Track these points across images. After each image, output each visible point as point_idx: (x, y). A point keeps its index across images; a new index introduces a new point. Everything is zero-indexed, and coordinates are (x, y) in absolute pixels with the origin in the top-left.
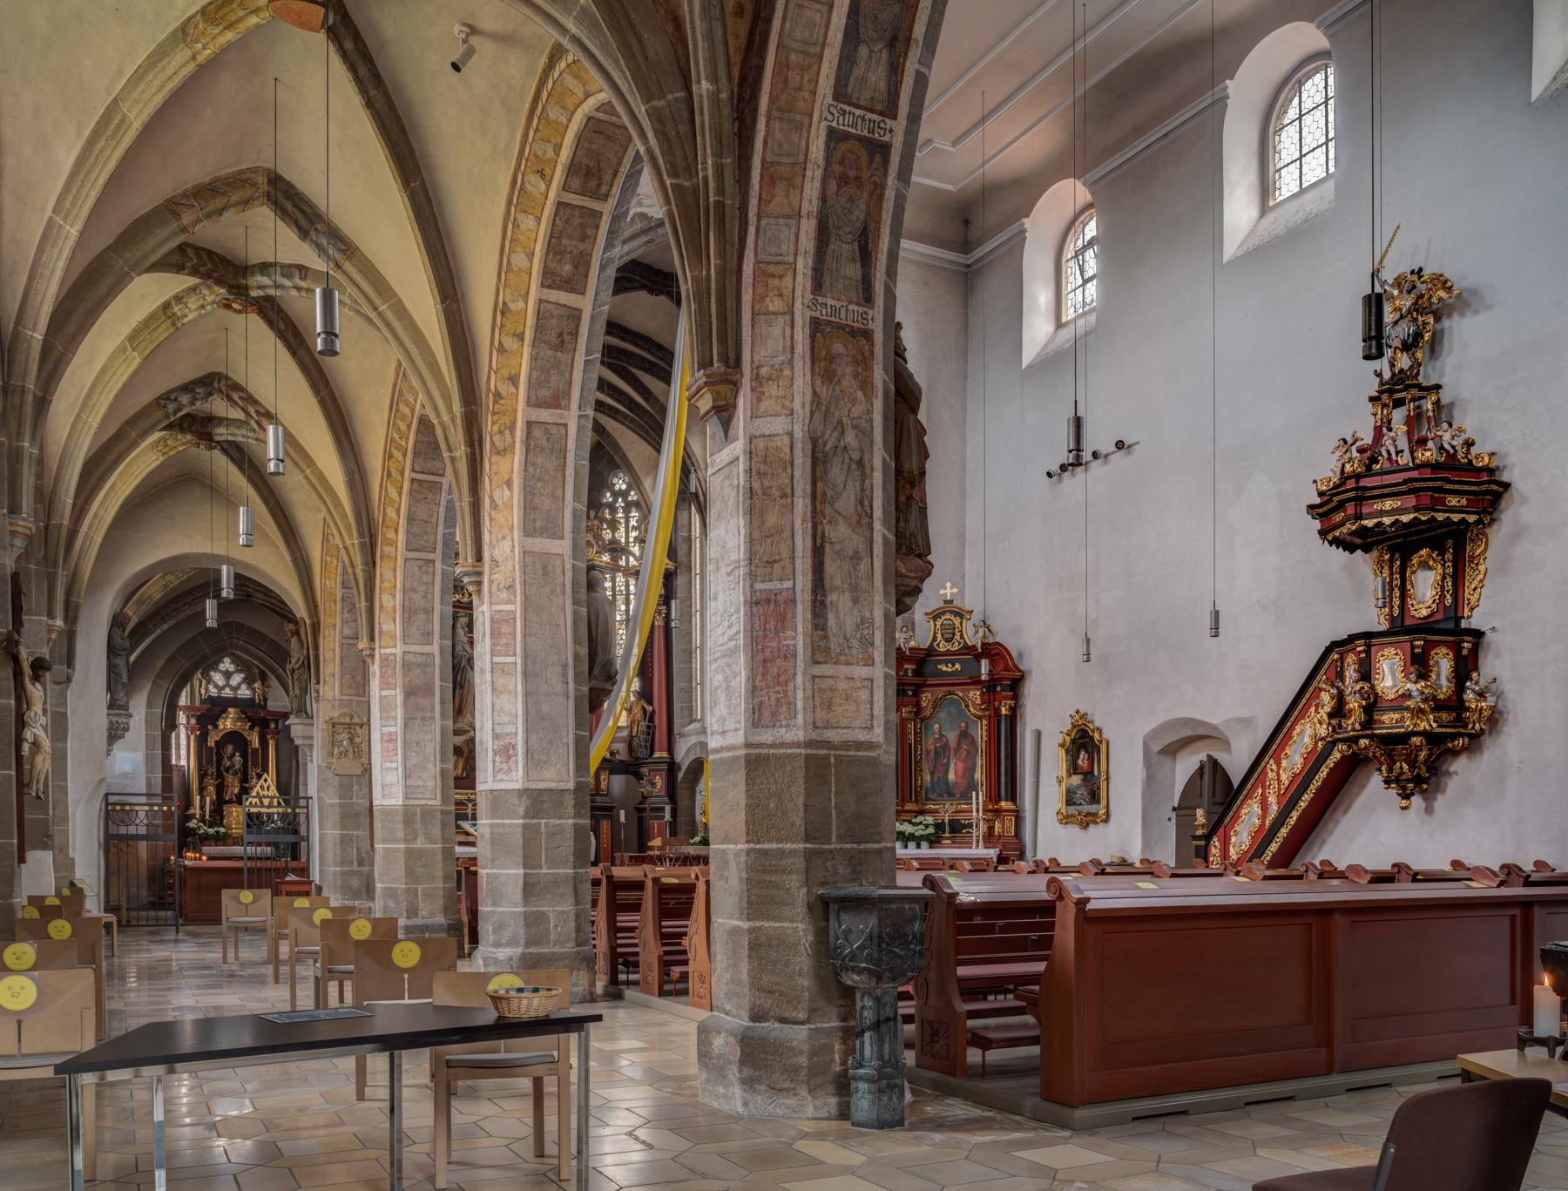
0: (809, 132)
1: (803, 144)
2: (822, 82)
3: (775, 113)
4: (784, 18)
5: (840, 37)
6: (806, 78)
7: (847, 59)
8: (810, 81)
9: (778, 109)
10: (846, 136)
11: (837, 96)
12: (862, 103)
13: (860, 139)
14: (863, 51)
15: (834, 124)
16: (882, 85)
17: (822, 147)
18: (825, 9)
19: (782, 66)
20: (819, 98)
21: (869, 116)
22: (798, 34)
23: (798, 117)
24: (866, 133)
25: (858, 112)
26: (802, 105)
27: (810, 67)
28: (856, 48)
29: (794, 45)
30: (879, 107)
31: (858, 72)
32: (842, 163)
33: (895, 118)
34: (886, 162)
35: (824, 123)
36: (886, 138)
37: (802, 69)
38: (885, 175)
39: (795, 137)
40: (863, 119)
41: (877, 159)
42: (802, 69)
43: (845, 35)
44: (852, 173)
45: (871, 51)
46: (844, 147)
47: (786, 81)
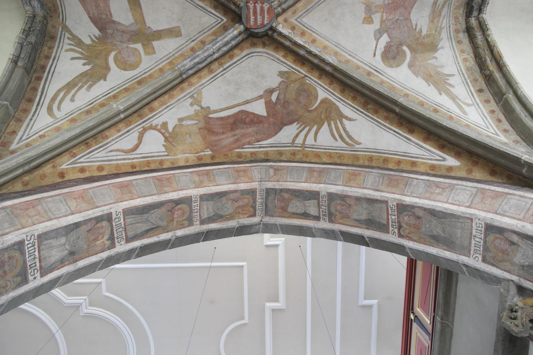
0: (16, 230)
1: (7, 231)
2: (42, 225)
3: (8, 210)
4: (50, 197)
5: (64, 224)
6: (37, 217)
7: (55, 233)
8: (37, 220)
9: (11, 211)
10: (23, 253)
11: (39, 236)
12: (42, 253)
13: (25, 262)
14: (63, 240)
15: (27, 242)
16: (53, 260)
17: (13, 241)
18: (70, 212)
19: (32, 205)
20: (34, 227)
21: (37, 260)
22: (50, 205)
23: (17, 222)
24: (29, 264)
25: (37, 253)
26: (24, 221)
27: (43, 217)
28: (63, 236)
29: (45, 206)
30: (43, 264)
31: (54, 242)
32: (10, 258)
33: (42, 276)
34: (19, 285)
35: (24, 237)
36: (31, 278)
37: (39, 214)
38: (14, 289)
39: (6, 225)
40: (35, 258)
41: (19, 279)
42: (39, 214)
43: (66, 227)
44: (7, 268)
45: (64, 244)
46: (17, 254)
47: (27, 209)
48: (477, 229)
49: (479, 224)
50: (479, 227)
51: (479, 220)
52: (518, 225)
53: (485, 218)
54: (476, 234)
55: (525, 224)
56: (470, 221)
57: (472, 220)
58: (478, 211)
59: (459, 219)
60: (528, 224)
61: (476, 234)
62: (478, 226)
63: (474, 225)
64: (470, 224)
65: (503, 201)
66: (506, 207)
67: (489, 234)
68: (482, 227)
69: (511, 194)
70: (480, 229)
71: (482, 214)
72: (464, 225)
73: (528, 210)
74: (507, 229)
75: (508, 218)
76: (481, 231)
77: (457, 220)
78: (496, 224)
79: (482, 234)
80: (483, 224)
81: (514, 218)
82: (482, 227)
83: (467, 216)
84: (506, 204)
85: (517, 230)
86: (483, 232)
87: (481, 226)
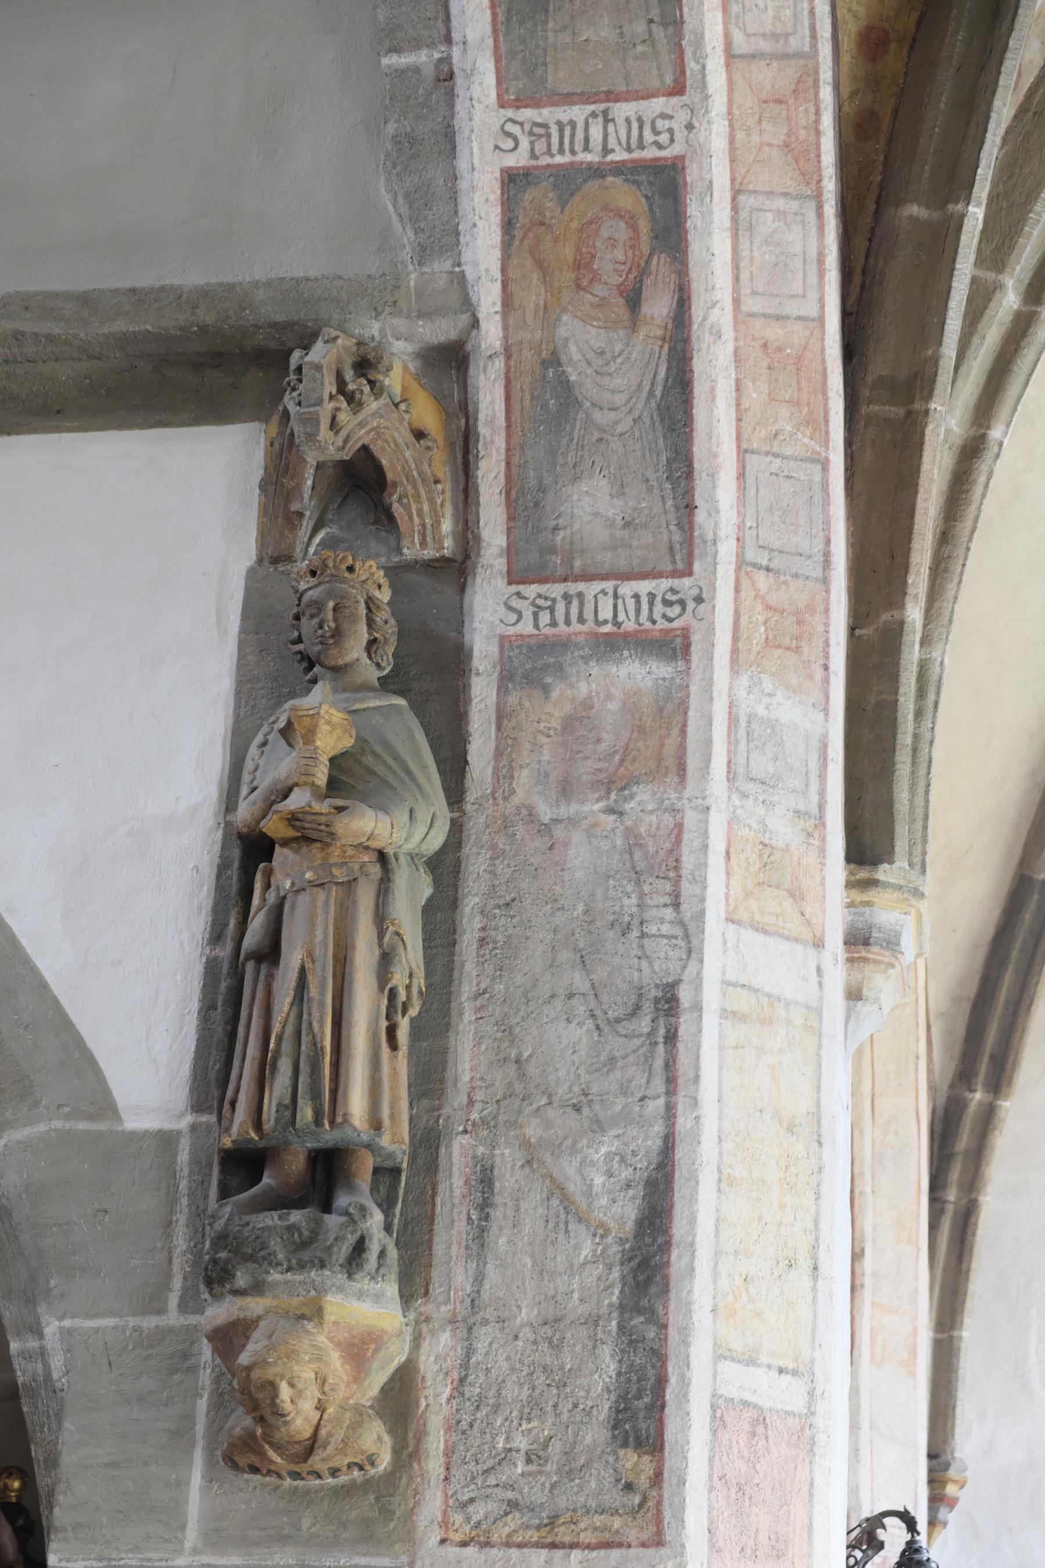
48: (640, 120)
49: (671, 131)
50: (656, 132)
51: (690, 127)
52: (716, 312)
53: (702, 152)
54: (621, 121)
55: (728, 333)
56: (669, 79)
57: (678, 89)
58: (724, 109)
59: (665, 25)
60: (730, 347)
61: (621, 121)
62: (660, 124)
63: (658, 104)
64: (656, 83)
65: (785, 195)
66: (767, 222)
67: (637, 184)
68: (660, 147)
69: (820, 215)
70: (648, 136)
71: (716, 137)
72: (644, 56)
73: (779, 318)
74: (685, 263)
75: (728, 255)
76: (641, 146)
77: (655, 13)
78: (693, 209)
79: (629, 149)
80: (677, 149)
81: (737, 279)
82: (660, 147)
83: (691, 66)
84: (780, 214)
85: (697, 311)
86: (637, 155)
87: (664, 138)
